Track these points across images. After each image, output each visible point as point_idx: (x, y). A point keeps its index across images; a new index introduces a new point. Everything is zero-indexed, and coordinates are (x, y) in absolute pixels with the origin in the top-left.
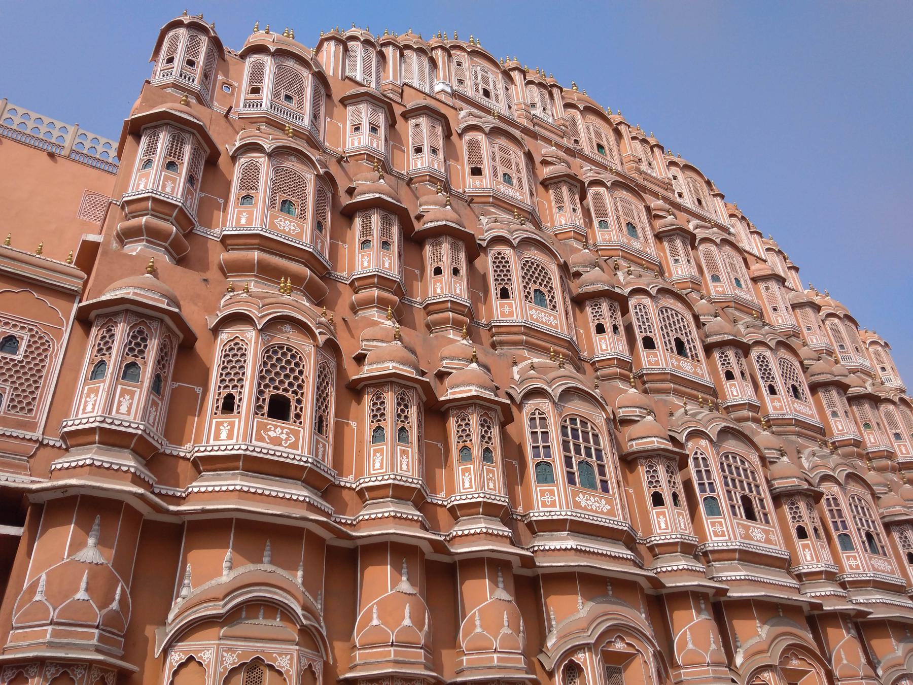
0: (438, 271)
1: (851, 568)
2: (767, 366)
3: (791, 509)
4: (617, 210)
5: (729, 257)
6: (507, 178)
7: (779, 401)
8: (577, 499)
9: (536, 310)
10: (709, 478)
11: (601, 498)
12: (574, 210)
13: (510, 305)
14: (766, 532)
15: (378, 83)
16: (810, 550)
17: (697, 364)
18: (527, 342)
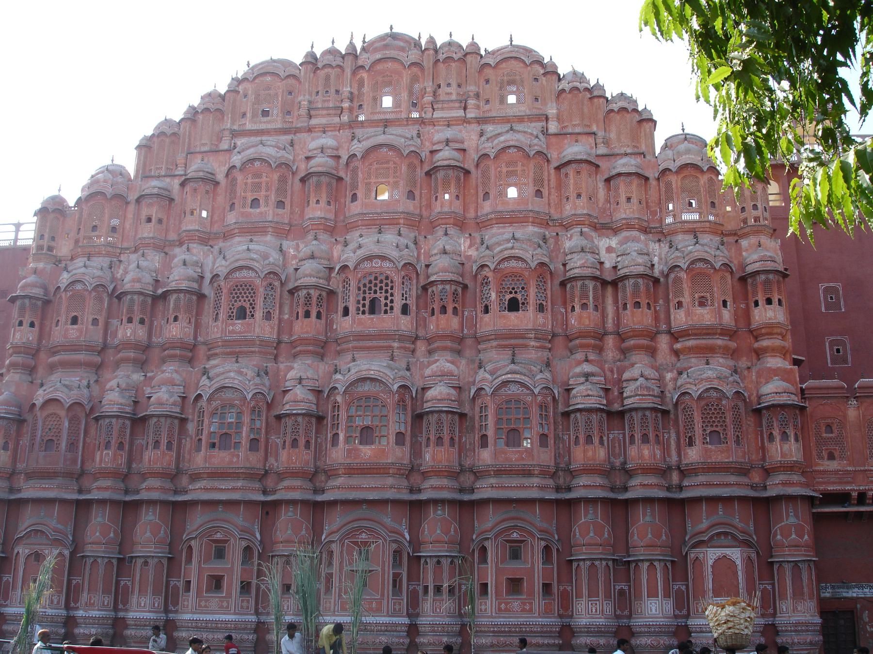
6: (255, 202)
12: (318, 202)
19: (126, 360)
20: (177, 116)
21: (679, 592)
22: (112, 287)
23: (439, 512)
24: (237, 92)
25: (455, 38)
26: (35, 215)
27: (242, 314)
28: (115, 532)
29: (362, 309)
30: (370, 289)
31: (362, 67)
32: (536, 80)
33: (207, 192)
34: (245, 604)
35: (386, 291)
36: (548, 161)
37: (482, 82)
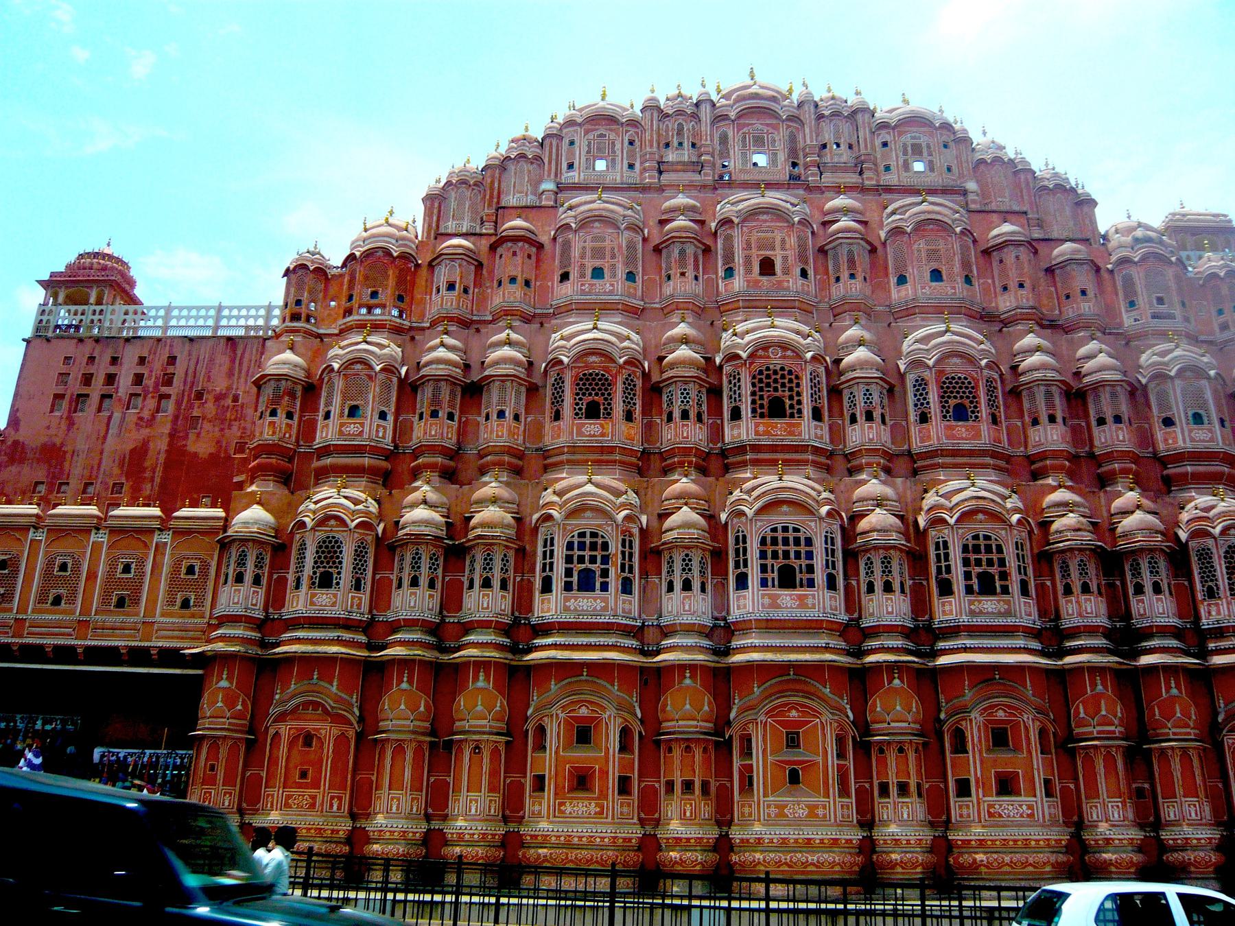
0: (487, 418)
2: (924, 389)
6: (598, 273)
15: (473, 220)
18: (569, 462)
19: (432, 467)
20: (478, 163)
21: (1140, 793)
22: (404, 370)
23: (896, 682)
25: (837, 94)
26: (287, 273)
27: (593, 412)
28: (427, 706)
31: (725, 117)
32: (945, 146)
33: (529, 256)
34: (625, 810)
35: (791, 389)
36: (975, 241)
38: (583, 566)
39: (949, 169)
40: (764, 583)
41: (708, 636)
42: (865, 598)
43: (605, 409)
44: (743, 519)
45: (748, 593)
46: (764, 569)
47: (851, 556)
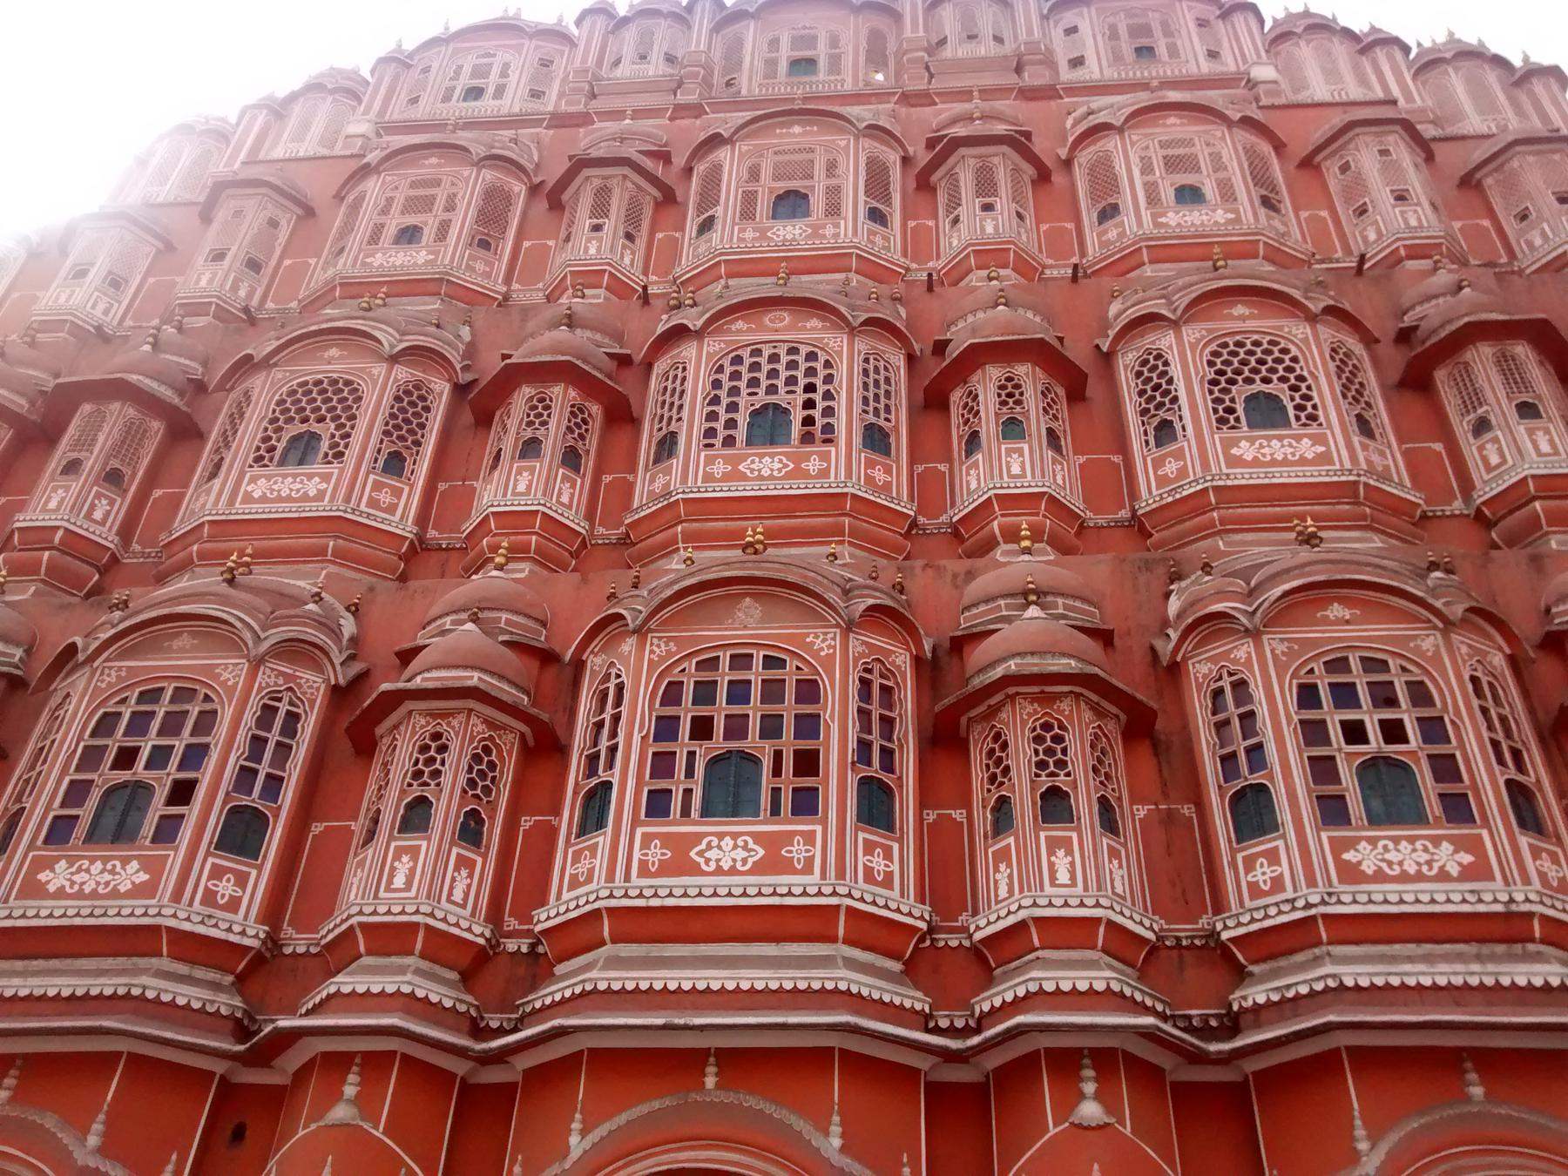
1: (1255, 891)
2: (1165, 373)
3: (991, 752)
4: (754, 174)
5: (1163, 145)
6: (409, 235)
7: (1179, 455)
8: (43, 877)
9: (268, 478)
10: (613, 734)
11: (125, 861)
12: (597, 228)
13: (208, 492)
14: (773, 843)
16: (1009, 865)
17: (825, 448)
18: (201, 556)
23: (1090, 1111)
24: (409, 66)
27: (302, 449)
29: (722, 433)
30: (754, 382)
33: (273, 223)
35: (810, 388)
37: (1057, 34)
38: (124, 776)
39: (1213, 55)
40: (658, 804)
41: (468, 979)
42: (985, 852)
43: (331, 448)
44: (629, 645)
45: (602, 840)
46: (663, 764)
47: (945, 739)
